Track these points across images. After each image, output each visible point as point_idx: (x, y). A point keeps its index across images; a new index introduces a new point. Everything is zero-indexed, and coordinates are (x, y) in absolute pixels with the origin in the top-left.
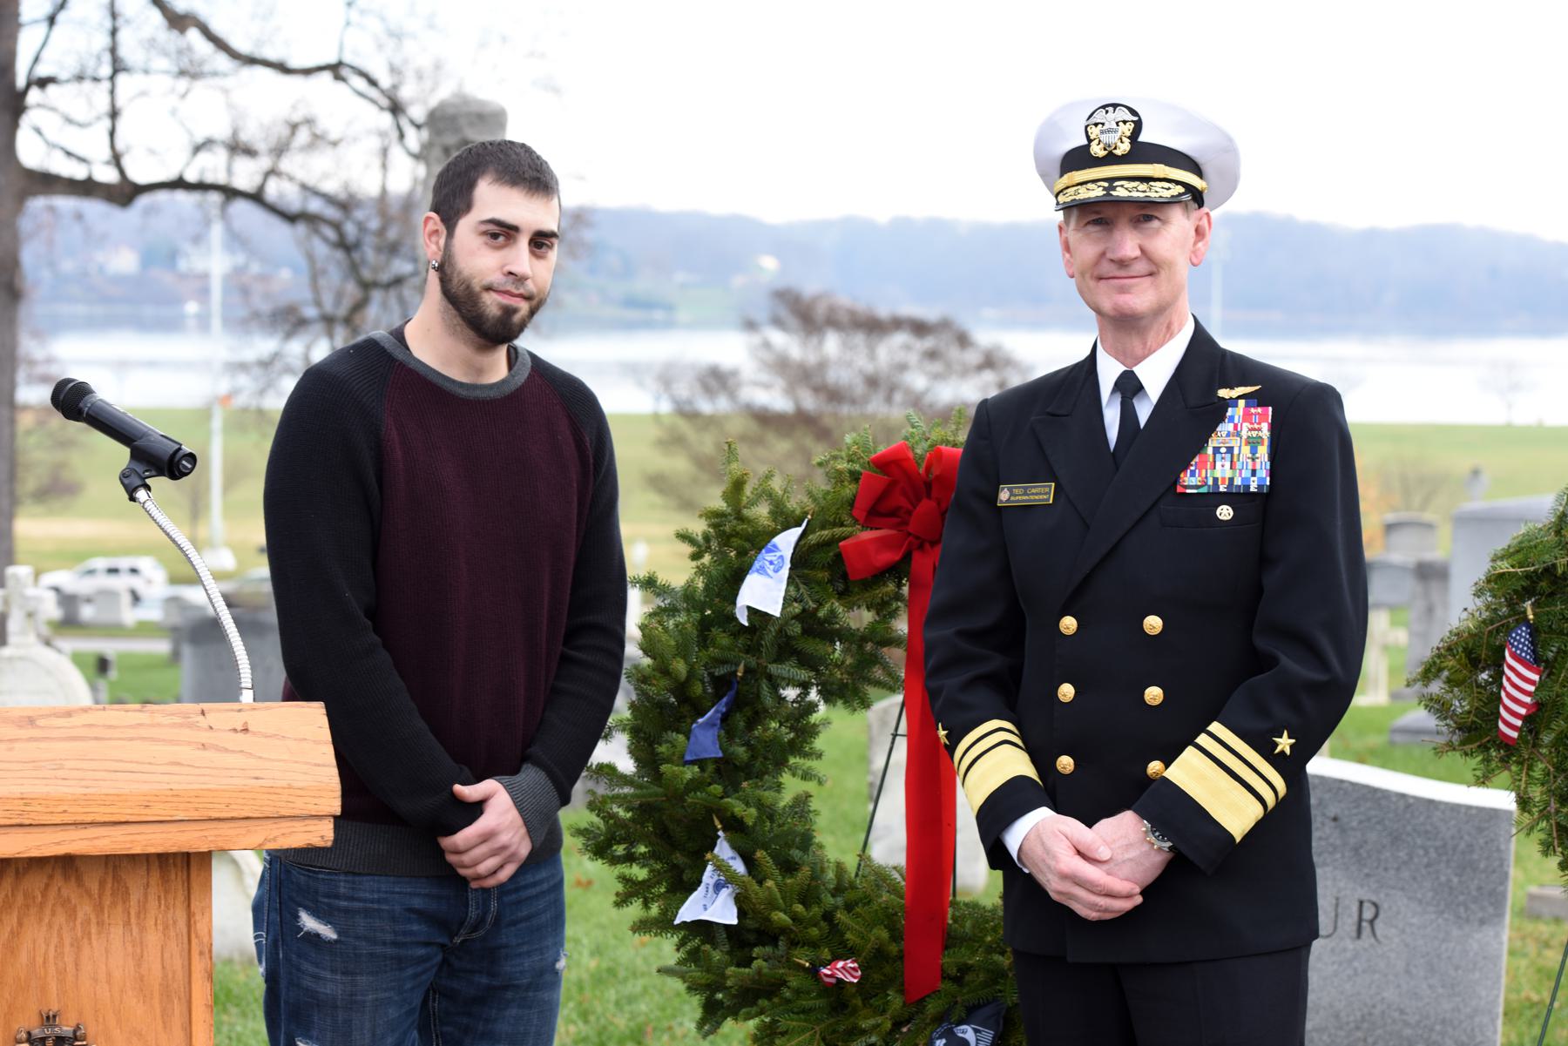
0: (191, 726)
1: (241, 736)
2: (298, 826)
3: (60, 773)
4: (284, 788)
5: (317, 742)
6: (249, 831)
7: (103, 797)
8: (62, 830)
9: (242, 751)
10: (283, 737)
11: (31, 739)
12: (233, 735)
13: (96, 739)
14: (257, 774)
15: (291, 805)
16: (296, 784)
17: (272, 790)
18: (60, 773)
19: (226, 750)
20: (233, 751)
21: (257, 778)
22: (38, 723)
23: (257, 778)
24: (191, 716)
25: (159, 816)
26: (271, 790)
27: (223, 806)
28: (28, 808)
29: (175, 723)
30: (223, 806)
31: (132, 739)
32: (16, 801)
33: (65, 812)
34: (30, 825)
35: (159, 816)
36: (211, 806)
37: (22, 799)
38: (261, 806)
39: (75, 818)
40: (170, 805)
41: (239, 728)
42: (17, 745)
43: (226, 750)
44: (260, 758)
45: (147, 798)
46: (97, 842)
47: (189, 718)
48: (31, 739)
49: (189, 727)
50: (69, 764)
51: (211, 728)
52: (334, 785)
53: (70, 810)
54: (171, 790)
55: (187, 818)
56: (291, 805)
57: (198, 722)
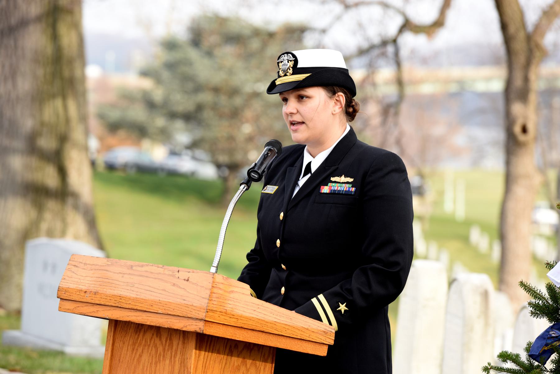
0: (173, 276)
1: (186, 282)
2: (194, 322)
3: (132, 288)
4: (190, 305)
5: (206, 289)
6: (180, 322)
7: (141, 300)
8: (130, 311)
9: (183, 288)
10: (198, 285)
11: (129, 274)
12: (184, 281)
13: (147, 277)
14: (185, 298)
15: (191, 313)
16: (195, 305)
17: (187, 306)
18: (132, 288)
19: (180, 287)
20: (181, 288)
21: (184, 300)
22: (134, 268)
23: (184, 300)
24: (175, 272)
25: (154, 310)
26: (187, 306)
27: (172, 310)
28: (120, 301)
29: (169, 274)
30: (172, 310)
31: (155, 278)
32: (118, 297)
33: (130, 304)
34: (120, 307)
35: (154, 310)
36: (169, 309)
37: (120, 296)
38: (183, 312)
39: (132, 307)
40: (158, 306)
41: (187, 279)
42: (125, 276)
43: (180, 287)
44: (188, 292)
45: (152, 302)
46: (138, 318)
47: (174, 273)
48: (129, 274)
49: (173, 276)
50: (136, 285)
51: (179, 278)
52: (205, 307)
53: (131, 303)
54: (159, 300)
55: (161, 313)
56: (191, 313)
57: (176, 275)
